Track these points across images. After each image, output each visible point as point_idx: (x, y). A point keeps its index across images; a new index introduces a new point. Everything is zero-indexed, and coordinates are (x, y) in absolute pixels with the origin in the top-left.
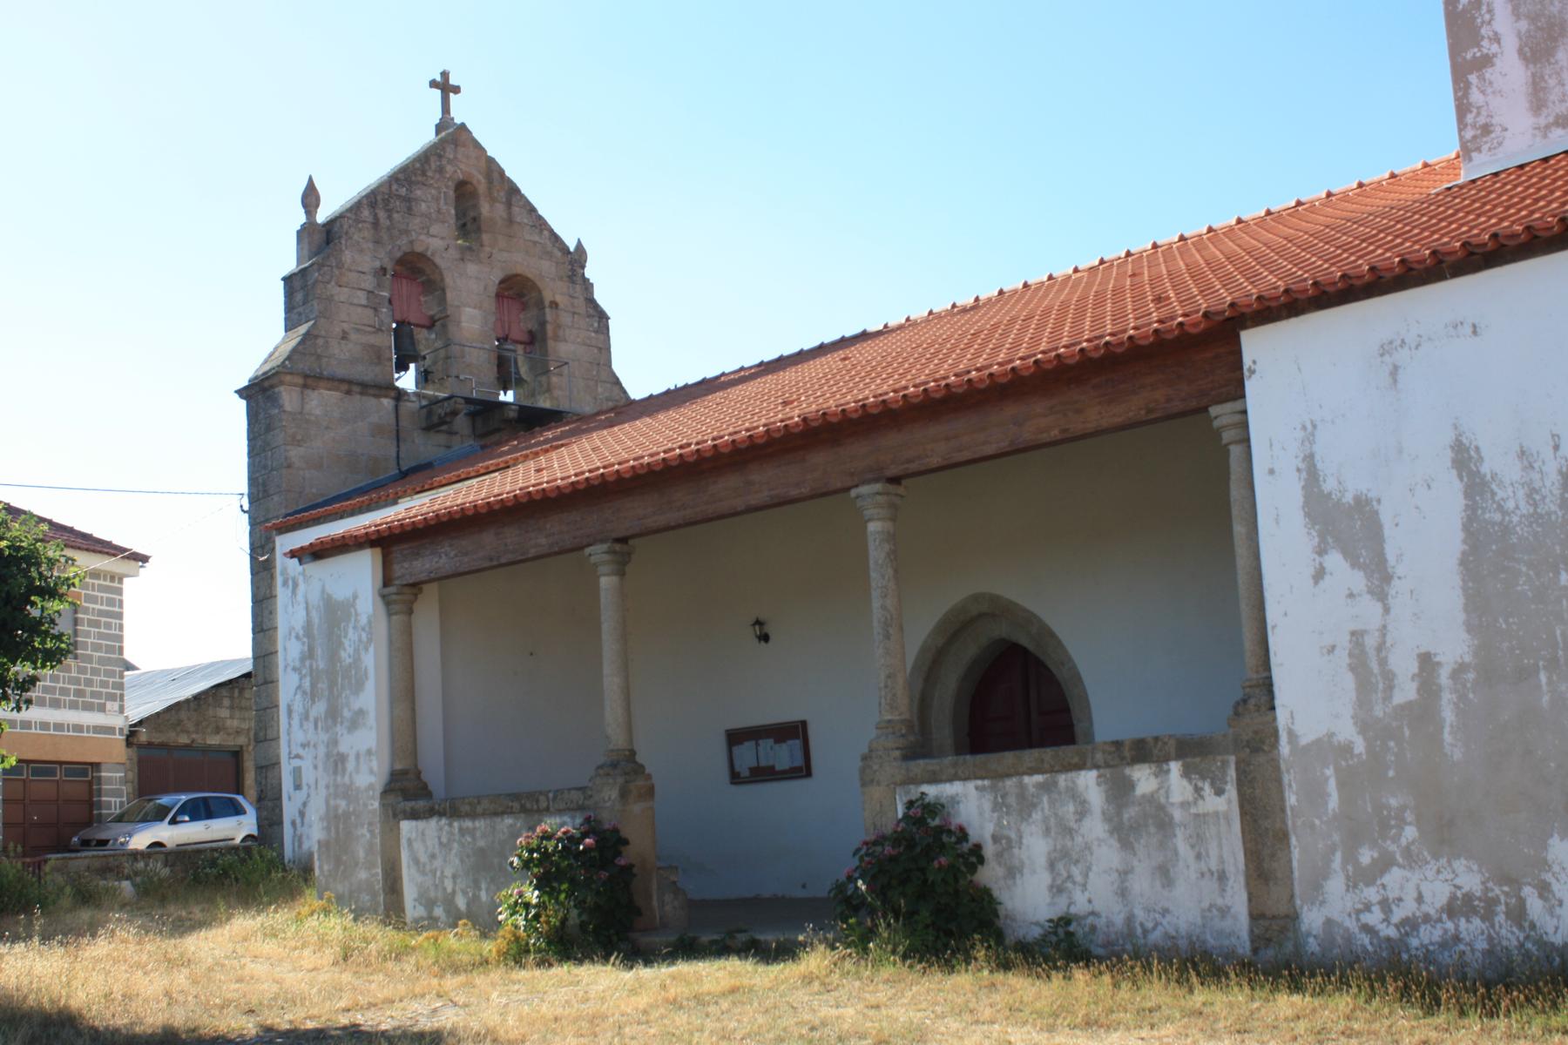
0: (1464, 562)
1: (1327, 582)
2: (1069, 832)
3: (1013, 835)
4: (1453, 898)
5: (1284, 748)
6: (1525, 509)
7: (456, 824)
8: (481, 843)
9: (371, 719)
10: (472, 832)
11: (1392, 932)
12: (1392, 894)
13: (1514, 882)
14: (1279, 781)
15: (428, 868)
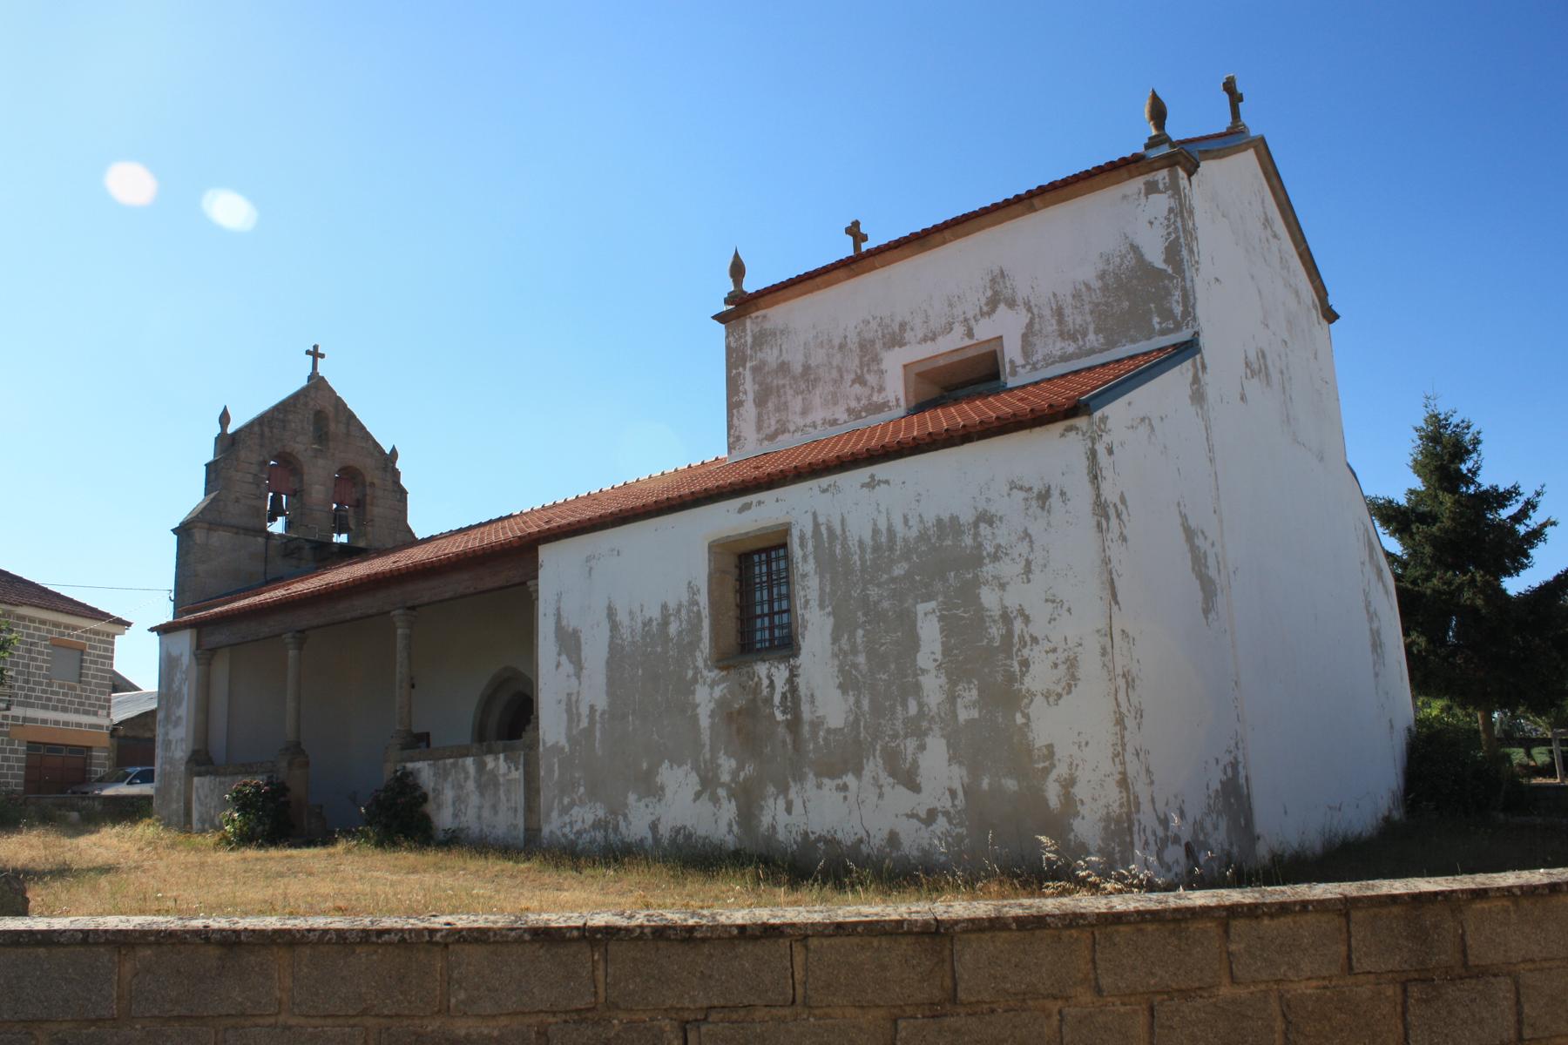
0: (607, 663)
1: (561, 669)
2: (461, 787)
3: (440, 788)
5: (541, 749)
6: (630, 639)
9: (184, 722)
11: (572, 837)
12: (574, 819)
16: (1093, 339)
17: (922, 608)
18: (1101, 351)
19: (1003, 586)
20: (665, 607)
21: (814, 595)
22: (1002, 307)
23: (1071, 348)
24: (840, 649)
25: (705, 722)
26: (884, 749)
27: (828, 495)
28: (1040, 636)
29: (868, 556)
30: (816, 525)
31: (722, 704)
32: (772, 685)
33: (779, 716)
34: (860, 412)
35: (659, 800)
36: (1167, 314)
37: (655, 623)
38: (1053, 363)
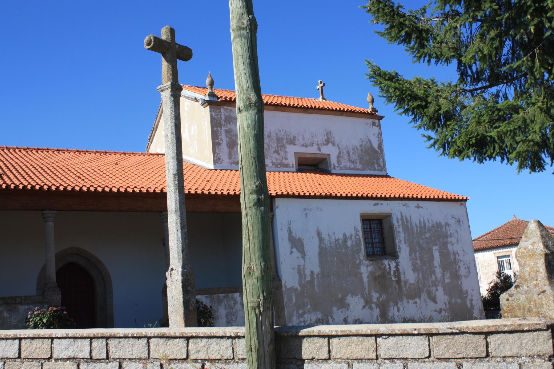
0: (319, 254)
2: (232, 308)
4: (317, 319)
5: (284, 289)
6: (329, 245)
12: (306, 319)
13: (327, 316)
14: (282, 296)
16: (359, 166)
17: (435, 248)
18: (361, 170)
19: (453, 245)
20: (345, 235)
21: (402, 239)
22: (330, 144)
23: (352, 166)
24: (412, 258)
25: (365, 279)
26: (427, 290)
27: (405, 207)
28: (461, 259)
29: (418, 229)
30: (402, 216)
31: (372, 274)
32: (390, 268)
33: (393, 279)
34: (278, 165)
35: (347, 309)
36: (379, 165)
37: (340, 241)
38: (347, 169)
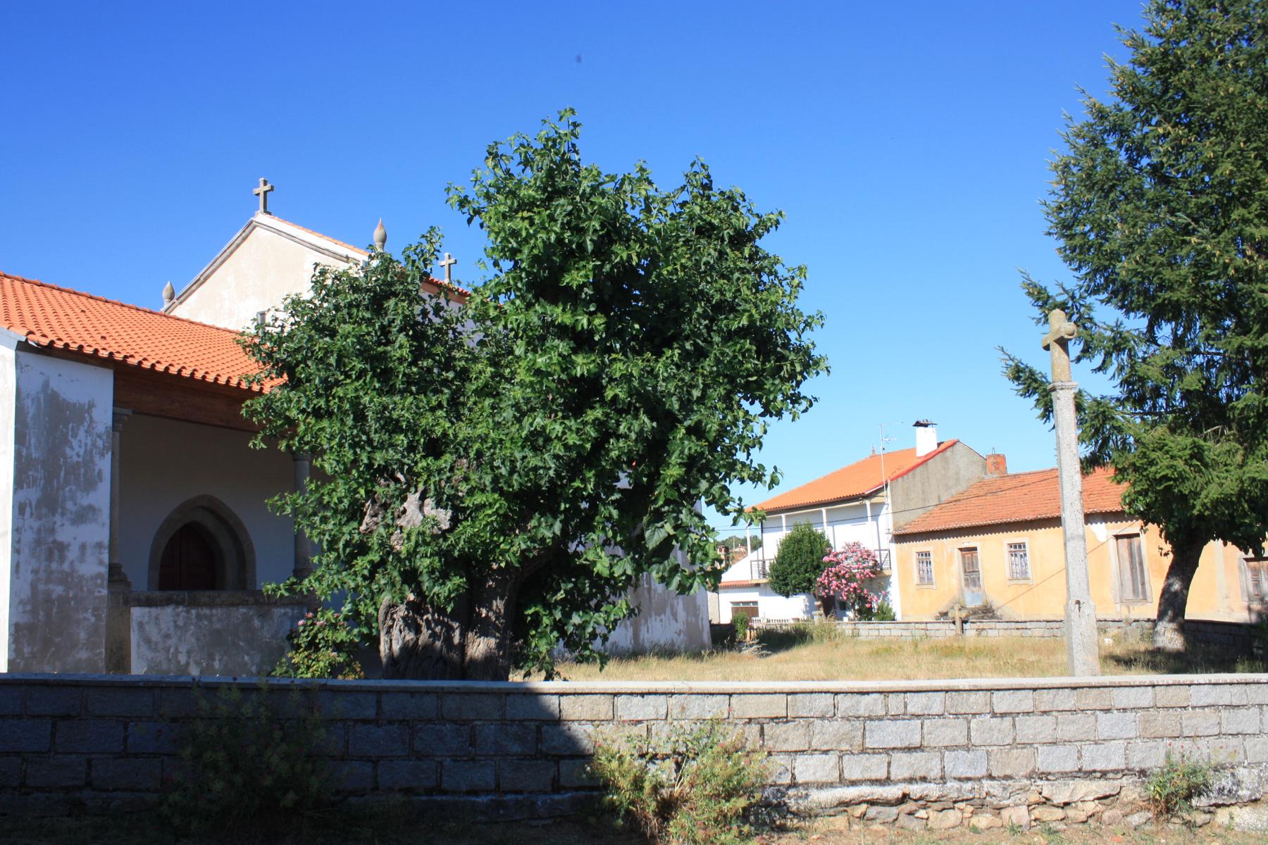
7: (194, 612)
8: (218, 626)
10: (209, 618)
15: (160, 646)
